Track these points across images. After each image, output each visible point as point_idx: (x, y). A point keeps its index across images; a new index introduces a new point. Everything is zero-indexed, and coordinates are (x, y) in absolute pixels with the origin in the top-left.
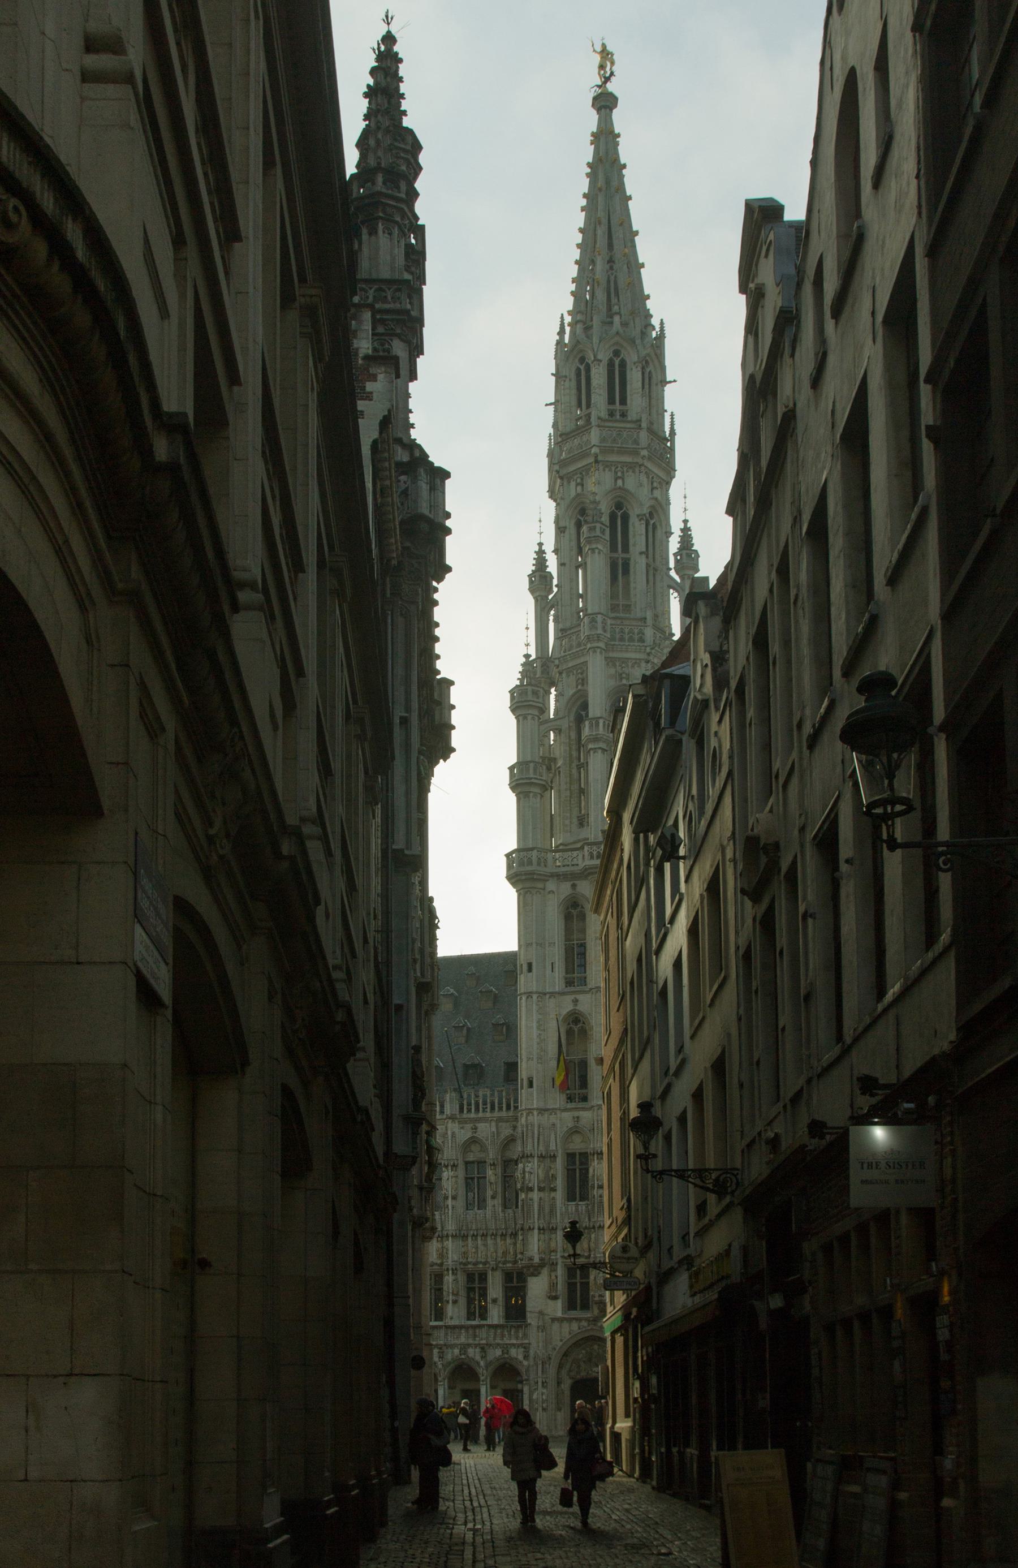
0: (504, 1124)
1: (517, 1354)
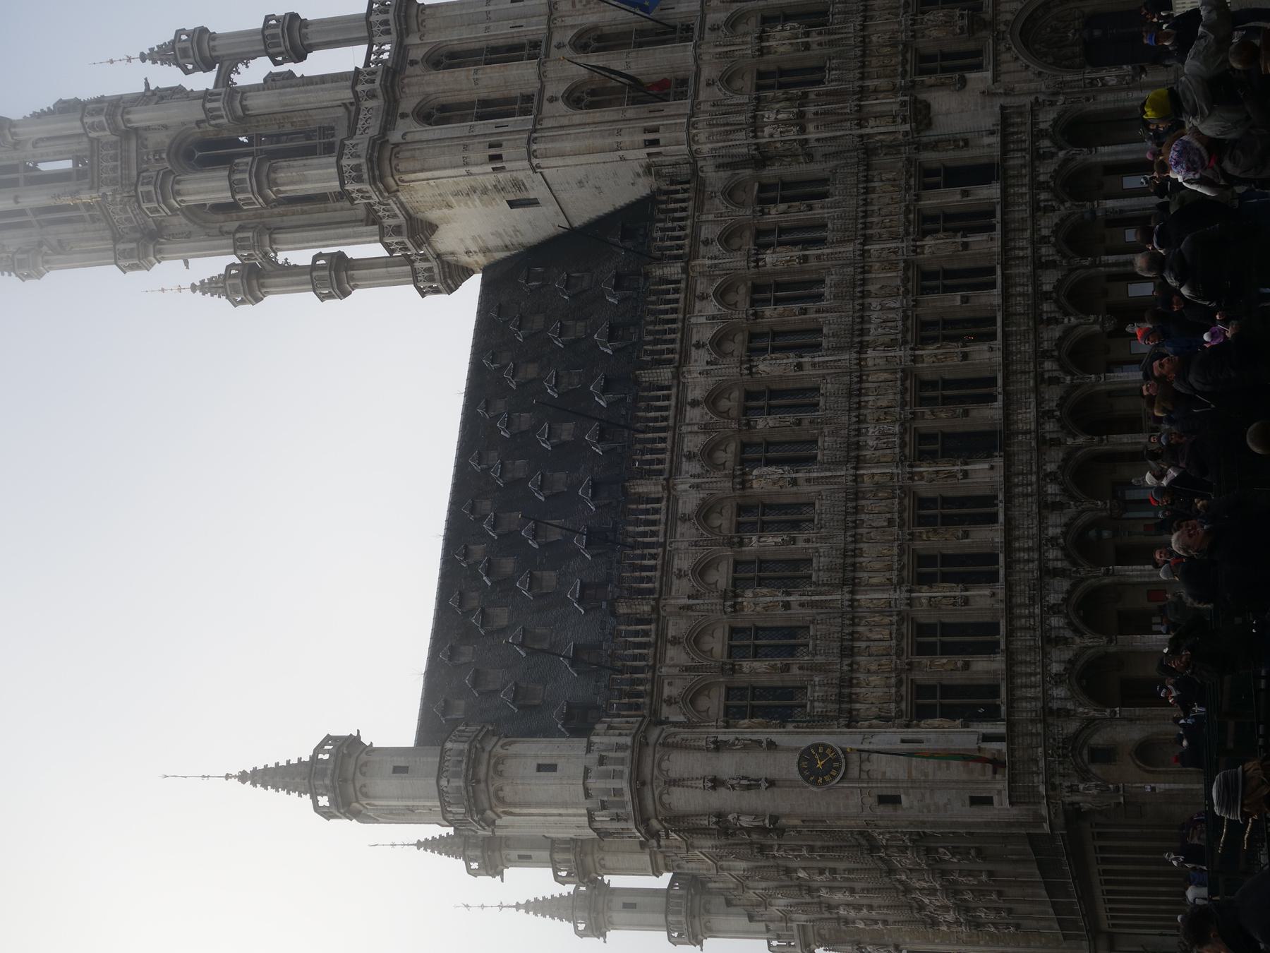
0: (706, 207)
1: (1047, 119)
